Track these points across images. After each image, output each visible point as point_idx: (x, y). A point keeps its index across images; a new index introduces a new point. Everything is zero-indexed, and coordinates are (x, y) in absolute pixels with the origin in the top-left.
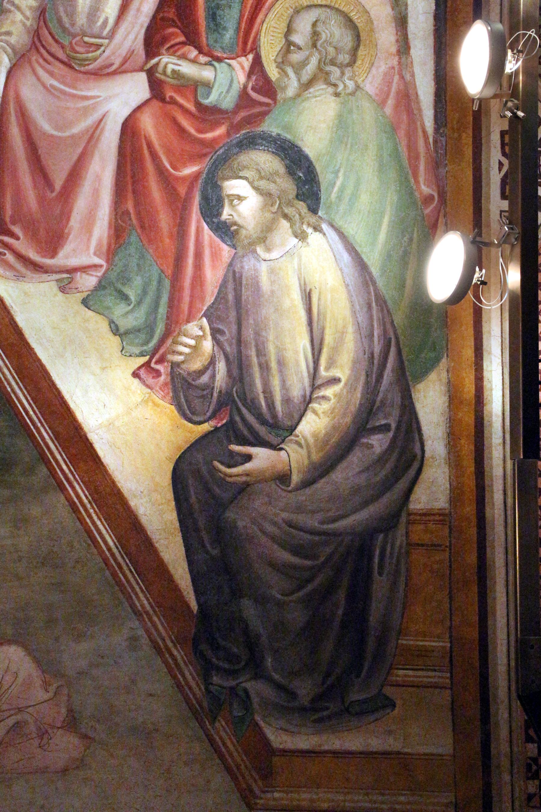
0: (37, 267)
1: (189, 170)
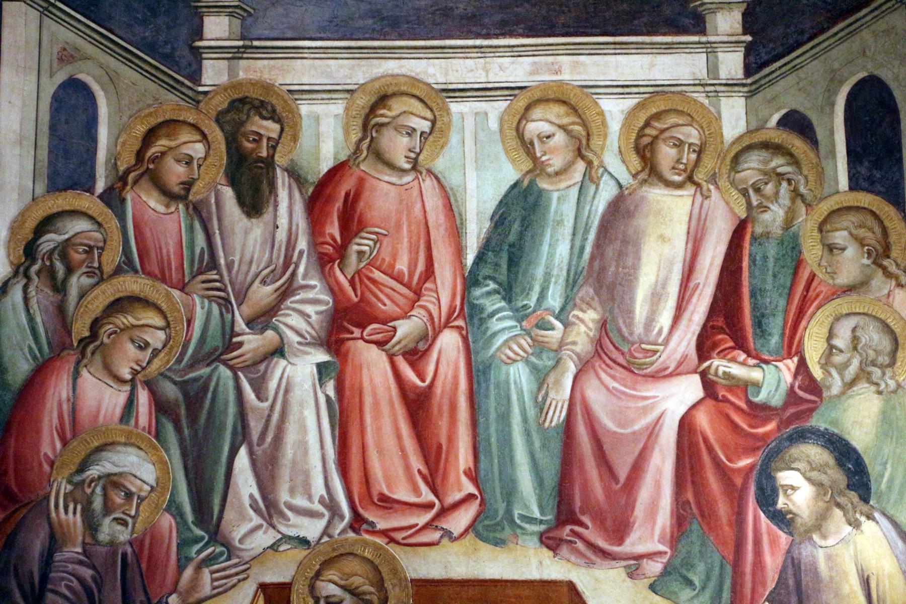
0: (605, 554)
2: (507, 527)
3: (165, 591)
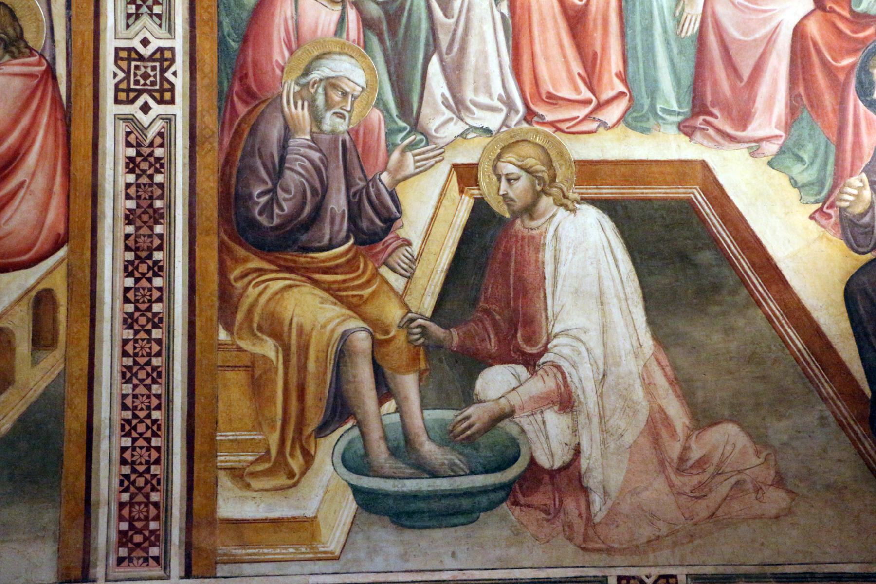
0: (731, 138)
1: (847, 62)
2: (651, 119)
3: (378, 170)
